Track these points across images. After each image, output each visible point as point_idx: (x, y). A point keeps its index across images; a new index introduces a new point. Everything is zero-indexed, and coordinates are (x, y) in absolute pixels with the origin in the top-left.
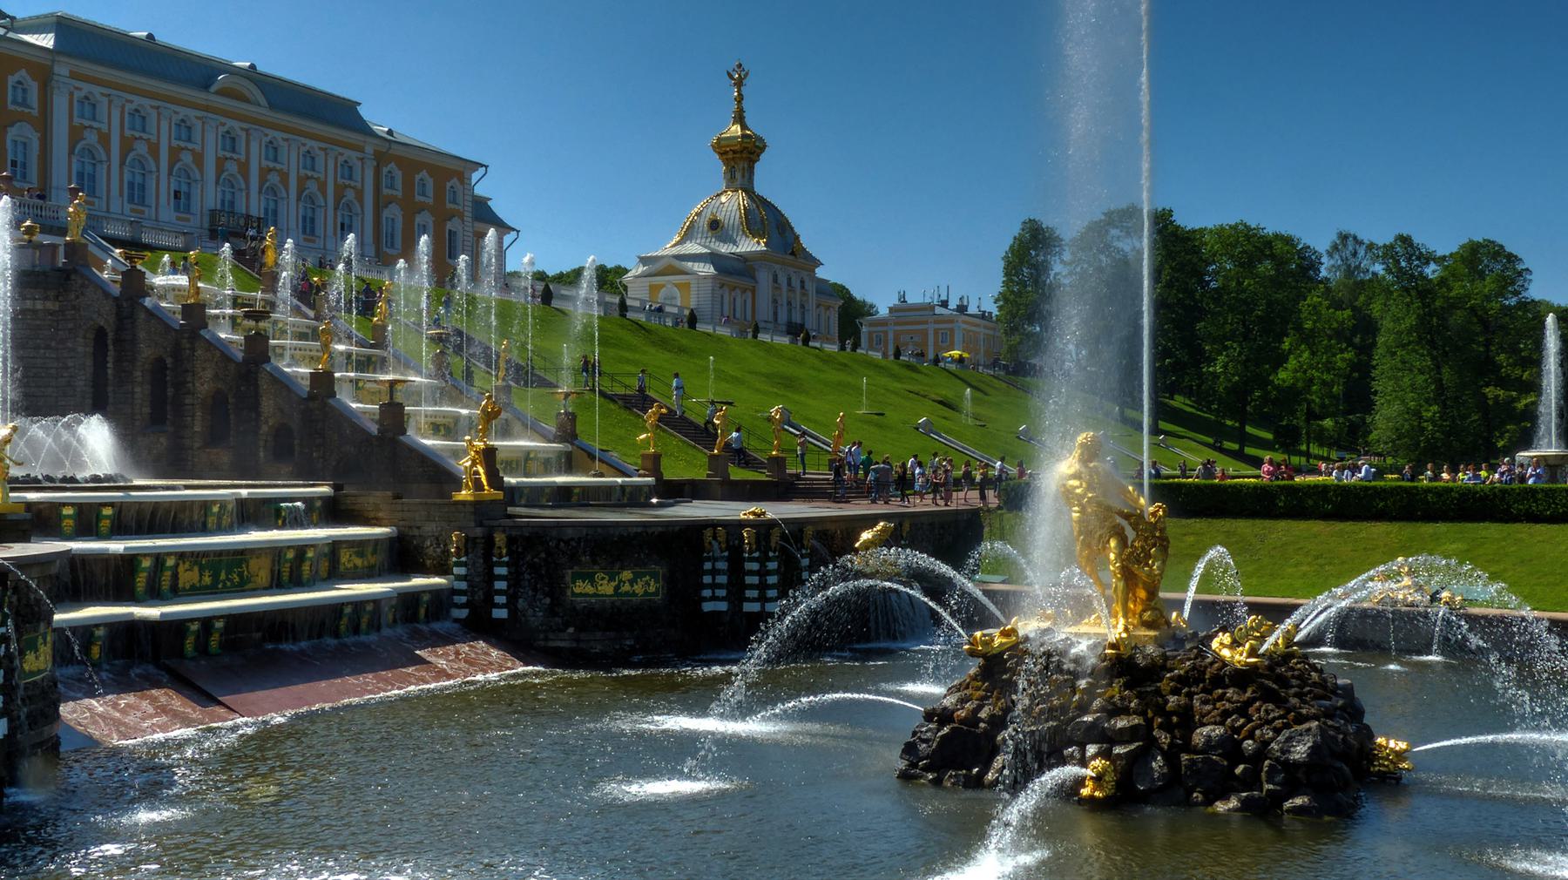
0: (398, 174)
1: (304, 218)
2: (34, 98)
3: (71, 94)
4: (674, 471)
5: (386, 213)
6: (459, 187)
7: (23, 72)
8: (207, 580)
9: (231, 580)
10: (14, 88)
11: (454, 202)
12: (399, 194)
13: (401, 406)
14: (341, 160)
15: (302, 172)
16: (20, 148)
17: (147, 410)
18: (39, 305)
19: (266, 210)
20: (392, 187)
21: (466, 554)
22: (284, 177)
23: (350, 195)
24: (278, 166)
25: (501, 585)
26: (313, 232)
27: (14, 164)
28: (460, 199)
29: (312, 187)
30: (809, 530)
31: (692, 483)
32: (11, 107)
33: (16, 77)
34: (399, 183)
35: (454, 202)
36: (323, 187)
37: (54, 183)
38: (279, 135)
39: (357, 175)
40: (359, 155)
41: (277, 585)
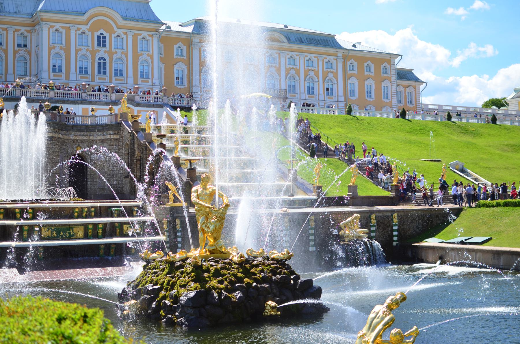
0: (355, 64)
1: (309, 88)
2: (185, 53)
5: (349, 81)
6: (388, 66)
7: (180, 43)
8: (55, 235)
9: (65, 235)
12: (356, 73)
13: (194, 169)
14: (325, 61)
15: (306, 68)
16: (180, 72)
18: (112, 137)
19: (290, 86)
22: (298, 71)
23: (331, 75)
24: (294, 67)
25: (179, 240)
26: (313, 93)
27: (178, 79)
29: (312, 74)
31: (341, 198)
32: (175, 57)
33: (178, 45)
34: (356, 68)
35: (386, 73)
36: (317, 74)
37: (194, 85)
38: (294, 54)
39: (334, 66)
40: (335, 58)
41: (86, 237)
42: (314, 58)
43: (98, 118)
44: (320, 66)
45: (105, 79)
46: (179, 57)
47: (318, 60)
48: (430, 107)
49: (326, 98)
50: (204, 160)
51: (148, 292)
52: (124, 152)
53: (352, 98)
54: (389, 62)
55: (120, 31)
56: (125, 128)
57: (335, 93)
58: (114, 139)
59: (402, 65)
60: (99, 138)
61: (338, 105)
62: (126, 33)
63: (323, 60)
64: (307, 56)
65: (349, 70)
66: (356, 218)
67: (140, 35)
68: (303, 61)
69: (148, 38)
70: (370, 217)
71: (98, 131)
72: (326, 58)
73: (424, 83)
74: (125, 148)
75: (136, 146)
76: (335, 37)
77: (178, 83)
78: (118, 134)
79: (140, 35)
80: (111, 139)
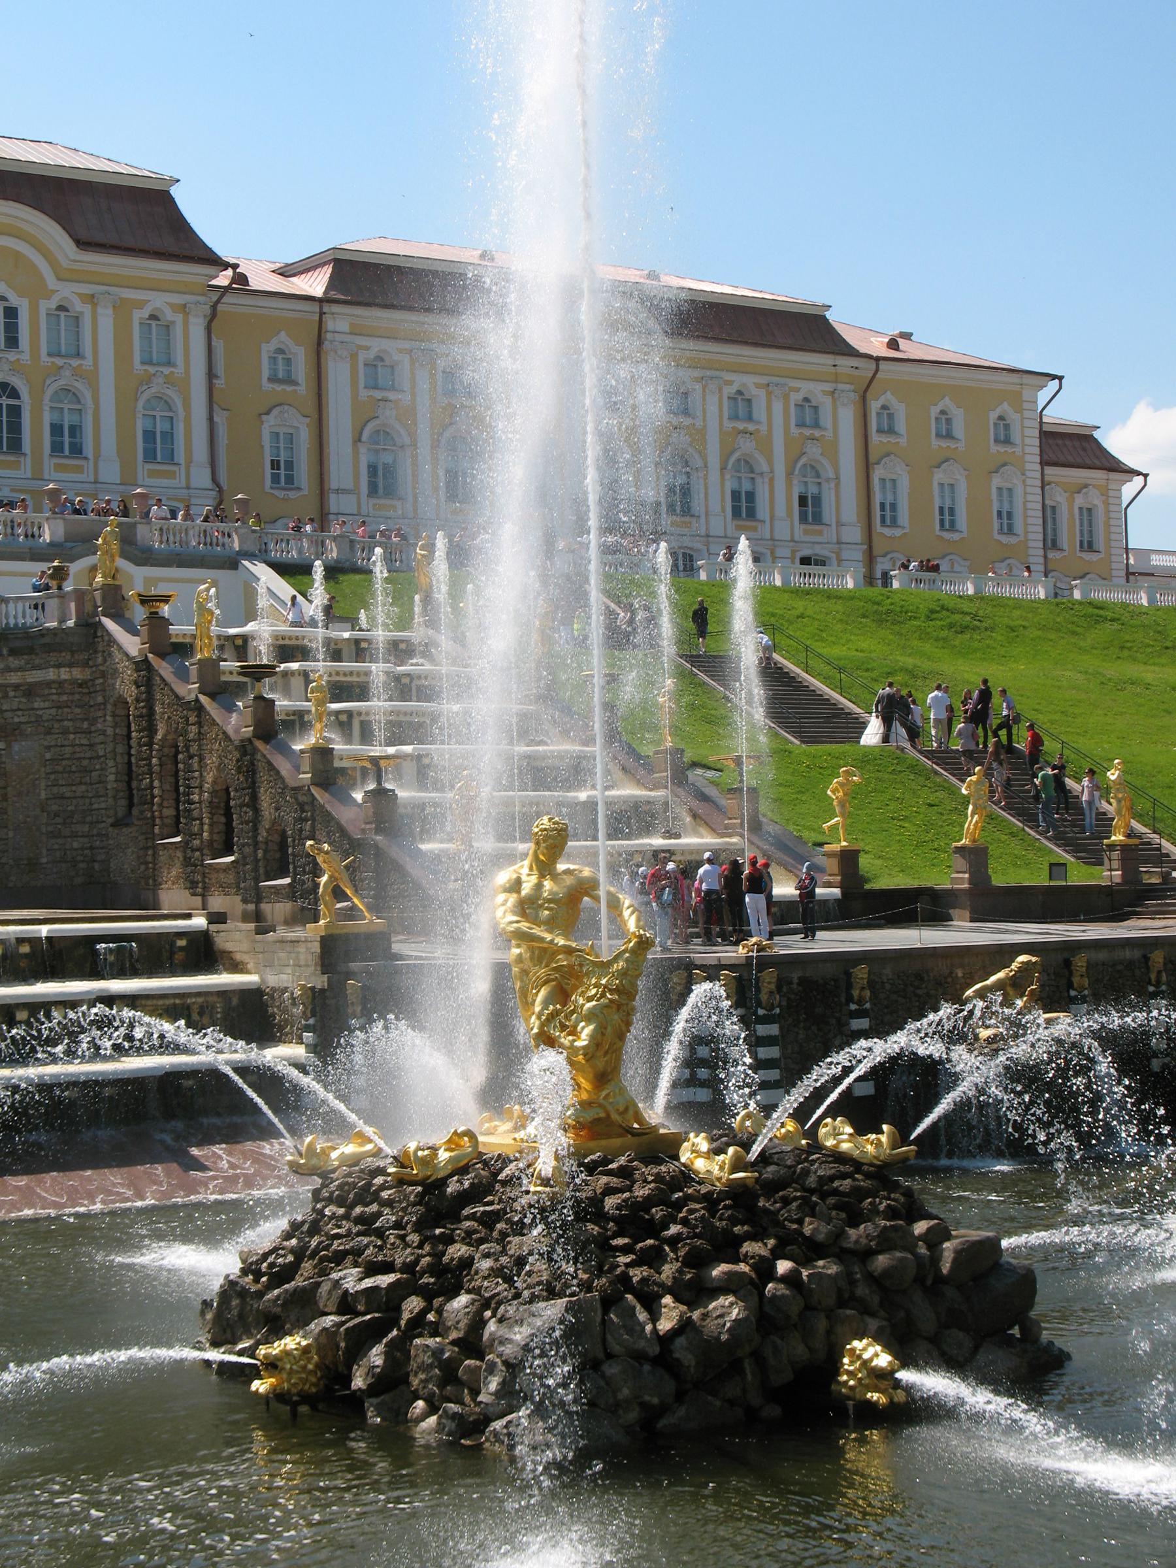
1: (736, 495)
3: (354, 357)
4: (885, 877)
5: (877, 474)
6: (1013, 417)
7: (283, 336)
10: (273, 360)
11: (1007, 441)
14: (795, 397)
15: (729, 425)
17: (169, 812)
18: (64, 674)
20: (891, 431)
21: (313, 1015)
23: (814, 450)
27: (275, 465)
28: (1016, 437)
30: (861, 973)
37: (334, 485)
39: (826, 419)
42: (755, 391)
43: (11, 605)
44: (775, 418)
45: (16, 466)
46: (279, 388)
47: (769, 394)
48: (1156, 561)
49: (799, 529)
50: (419, 757)
51: (346, 1305)
52: (110, 731)
53: (887, 531)
54: (1019, 401)
55: (67, 292)
56: (111, 641)
57: (828, 514)
58: (74, 682)
59: (1064, 409)
60: (14, 678)
61: (838, 554)
62: (91, 299)
63: (786, 397)
64: (729, 383)
65: (880, 431)
66: (1026, 968)
67: (141, 304)
68: (716, 399)
69: (169, 315)
70: (1067, 964)
71: (13, 652)
72: (798, 390)
73: (1139, 473)
74: (114, 715)
75: (158, 709)
76: (828, 315)
77: (275, 479)
78: (85, 664)
79: (141, 304)
80: (60, 683)
